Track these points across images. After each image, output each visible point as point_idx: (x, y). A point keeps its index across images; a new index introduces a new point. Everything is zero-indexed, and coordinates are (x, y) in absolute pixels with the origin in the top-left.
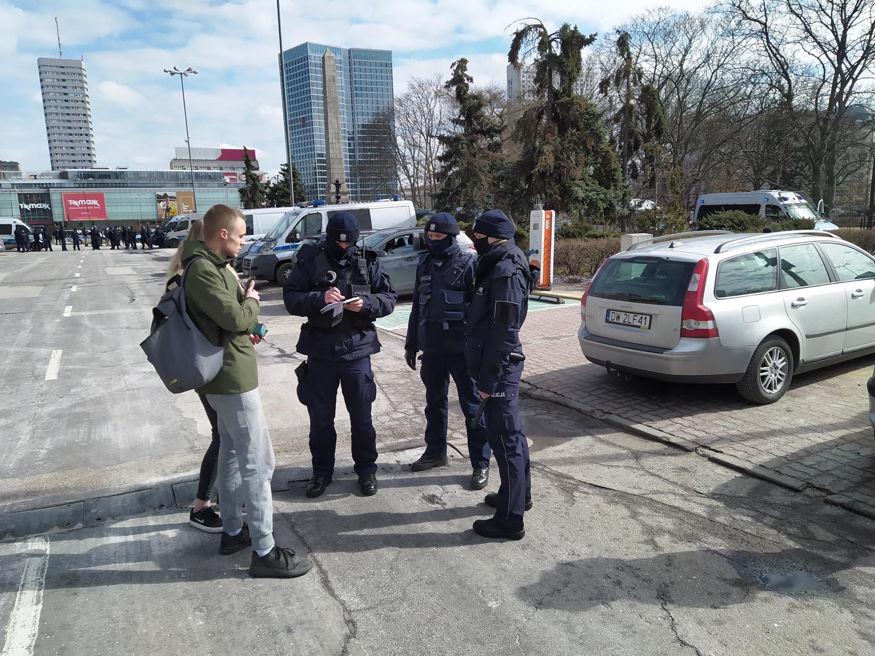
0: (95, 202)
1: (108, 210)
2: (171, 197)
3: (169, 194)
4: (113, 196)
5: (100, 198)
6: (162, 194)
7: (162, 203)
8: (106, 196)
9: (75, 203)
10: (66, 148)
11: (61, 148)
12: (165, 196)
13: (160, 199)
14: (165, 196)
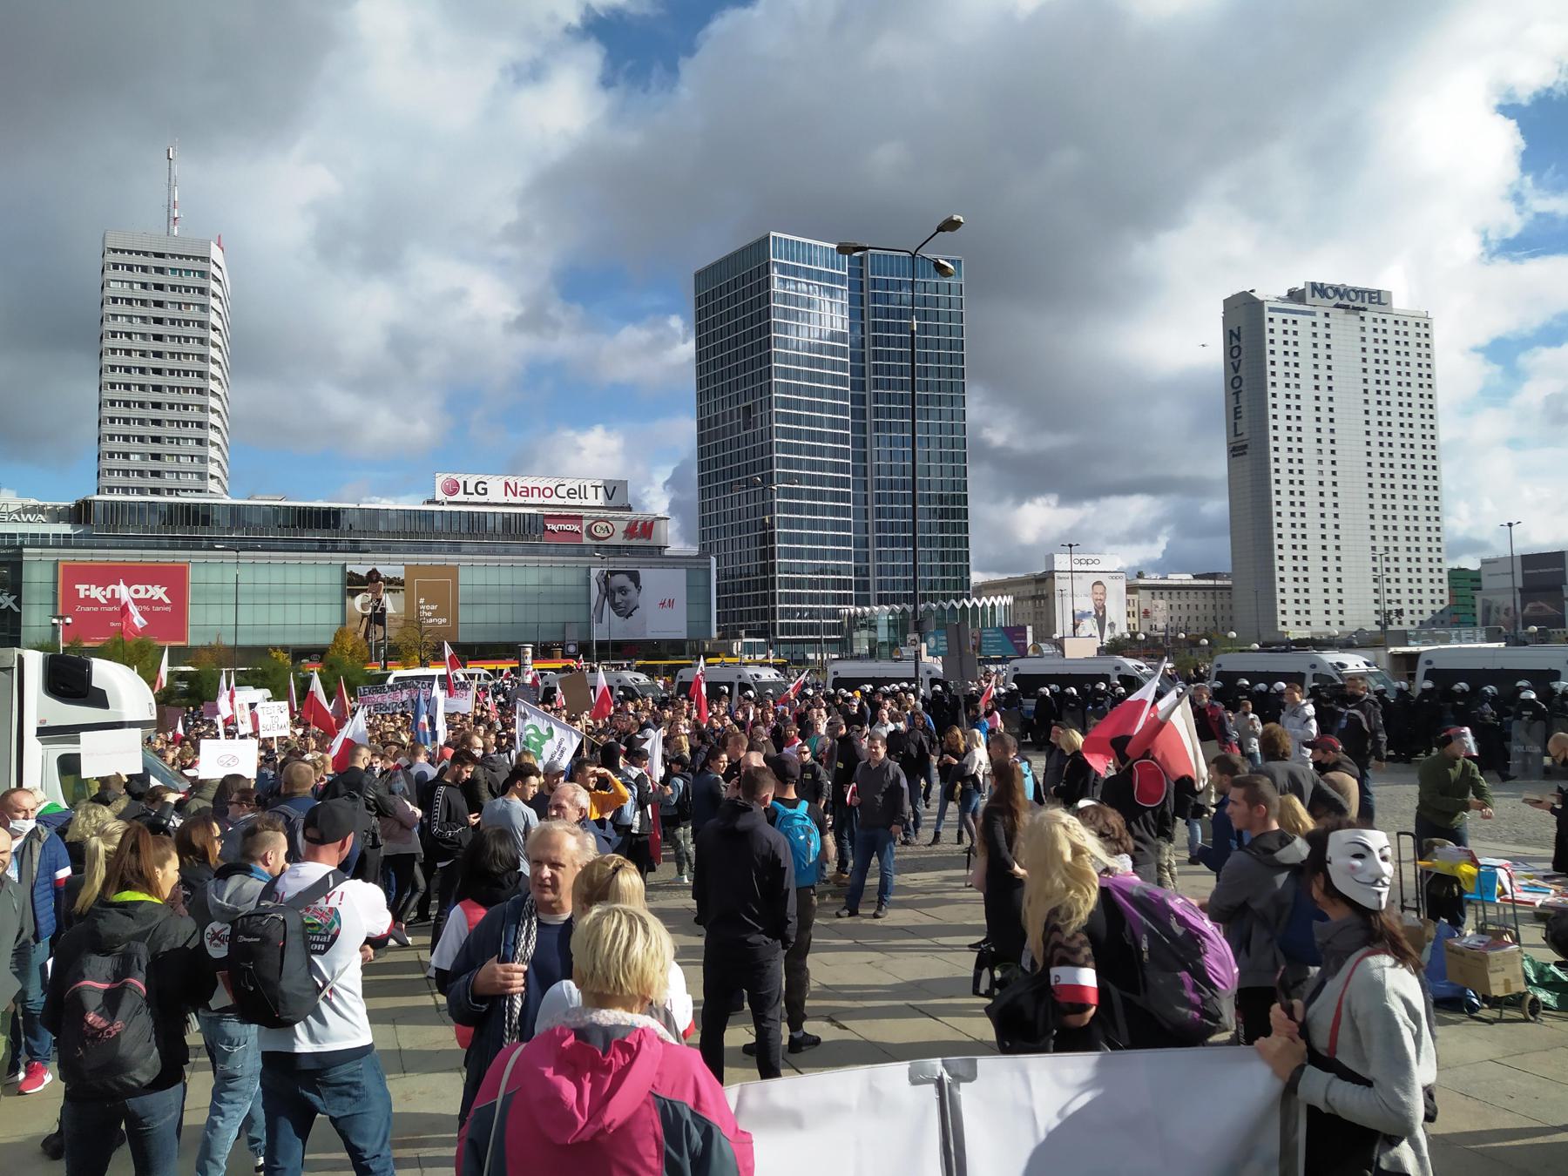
0: (158, 592)
1: (195, 615)
2: (390, 581)
3: (385, 571)
4: (214, 575)
5: (175, 580)
6: (362, 571)
7: (359, 599)
8: (193, 575)
9: (96, 592)
10: (143, 456)
11: (126, 456)
12: (373, 576)
13: (354, 585)
14: (373, 576)
